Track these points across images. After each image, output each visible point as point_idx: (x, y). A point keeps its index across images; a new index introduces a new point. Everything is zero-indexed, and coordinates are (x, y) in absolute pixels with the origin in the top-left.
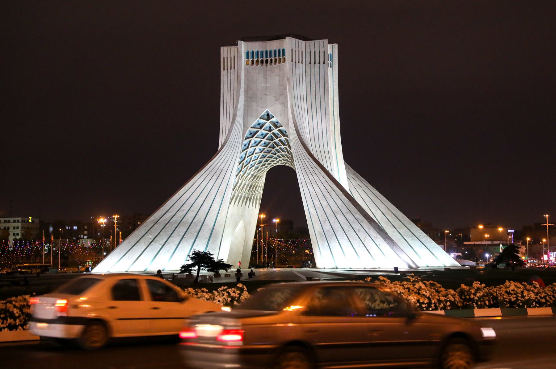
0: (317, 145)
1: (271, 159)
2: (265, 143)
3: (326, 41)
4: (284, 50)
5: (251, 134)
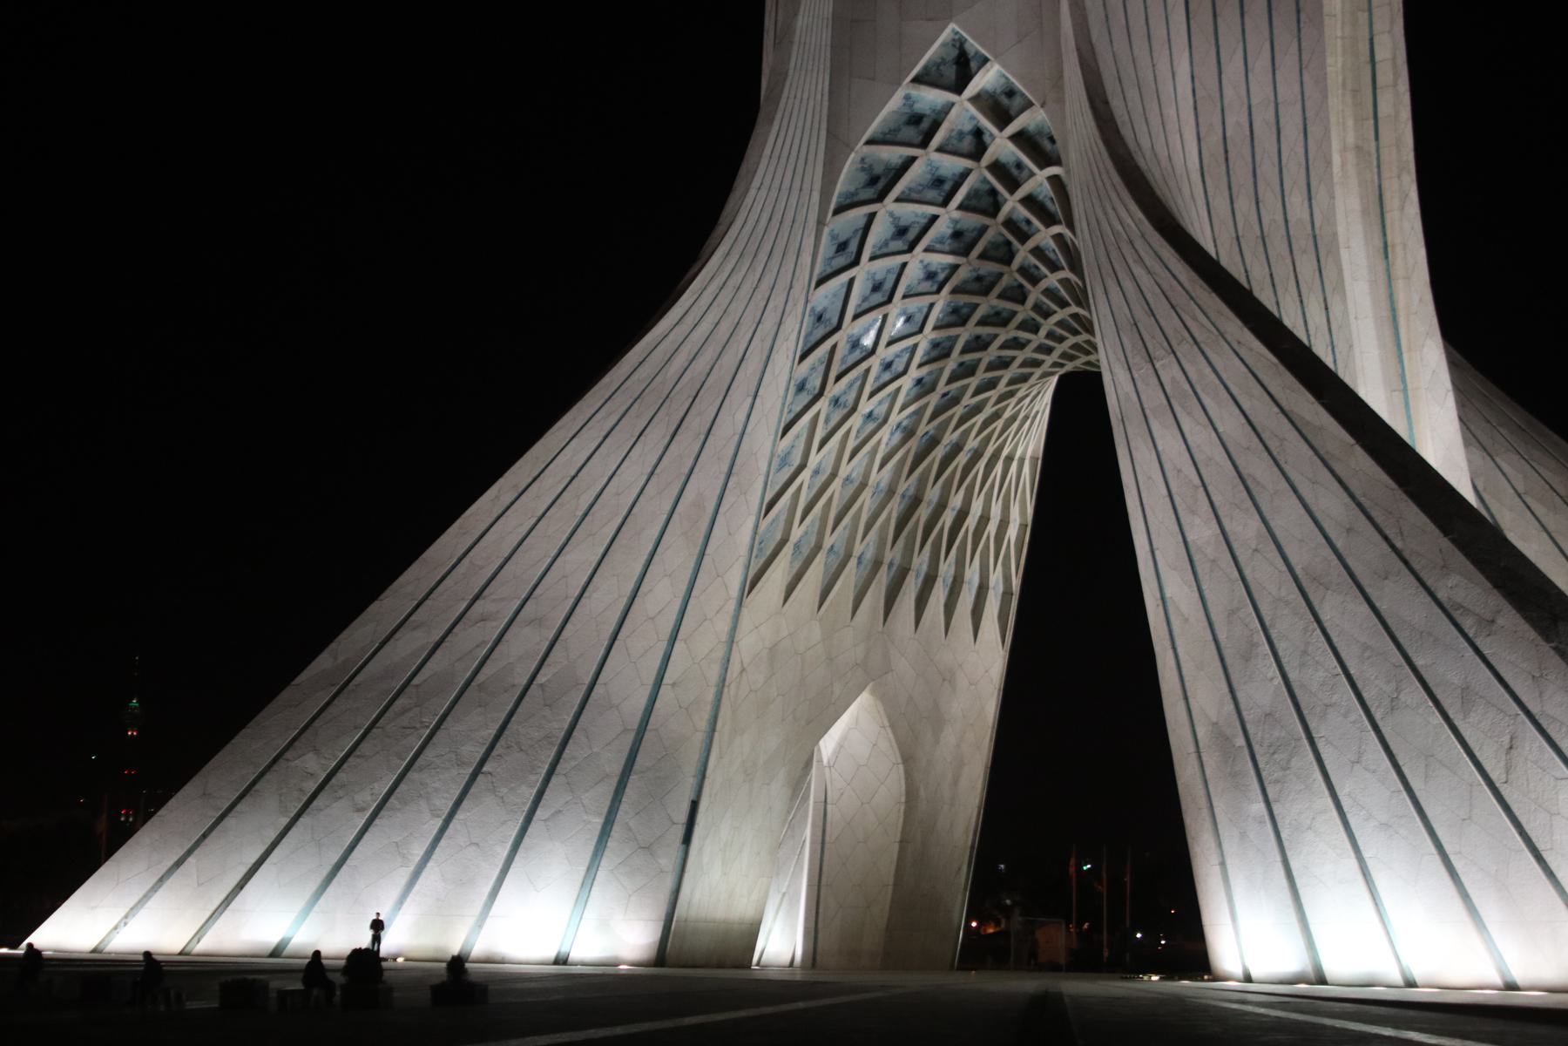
0: (1244, 204)
1: (1004, 335)
2: (957, 235)
5: (873, 181)
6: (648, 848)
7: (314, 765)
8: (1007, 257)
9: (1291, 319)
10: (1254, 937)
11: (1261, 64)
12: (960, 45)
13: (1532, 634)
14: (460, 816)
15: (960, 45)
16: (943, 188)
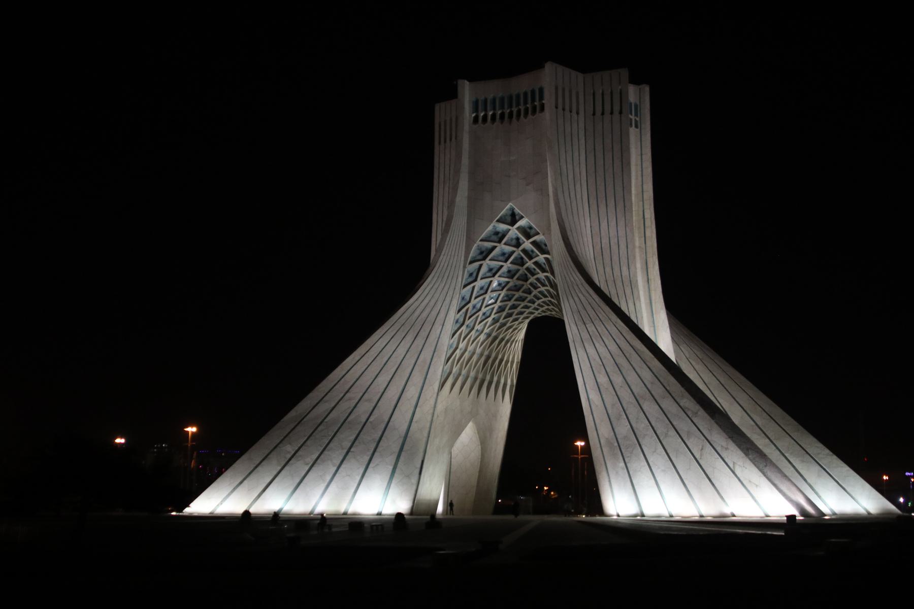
0: (608, 269)
1: (523, 304)
2: (509, 271)
3: (625, 73)
4: (541, 90)
5: (481, 253)
6: (408, 476)
7: (290, 449)
8: (526, 280)
9: (624, 308)
10: (620, 503)
11: (613, 223)
12: (512, 210)
13: (708, 417)
14: (343, 466)
15: (512, 210)
16: (506, 257)
